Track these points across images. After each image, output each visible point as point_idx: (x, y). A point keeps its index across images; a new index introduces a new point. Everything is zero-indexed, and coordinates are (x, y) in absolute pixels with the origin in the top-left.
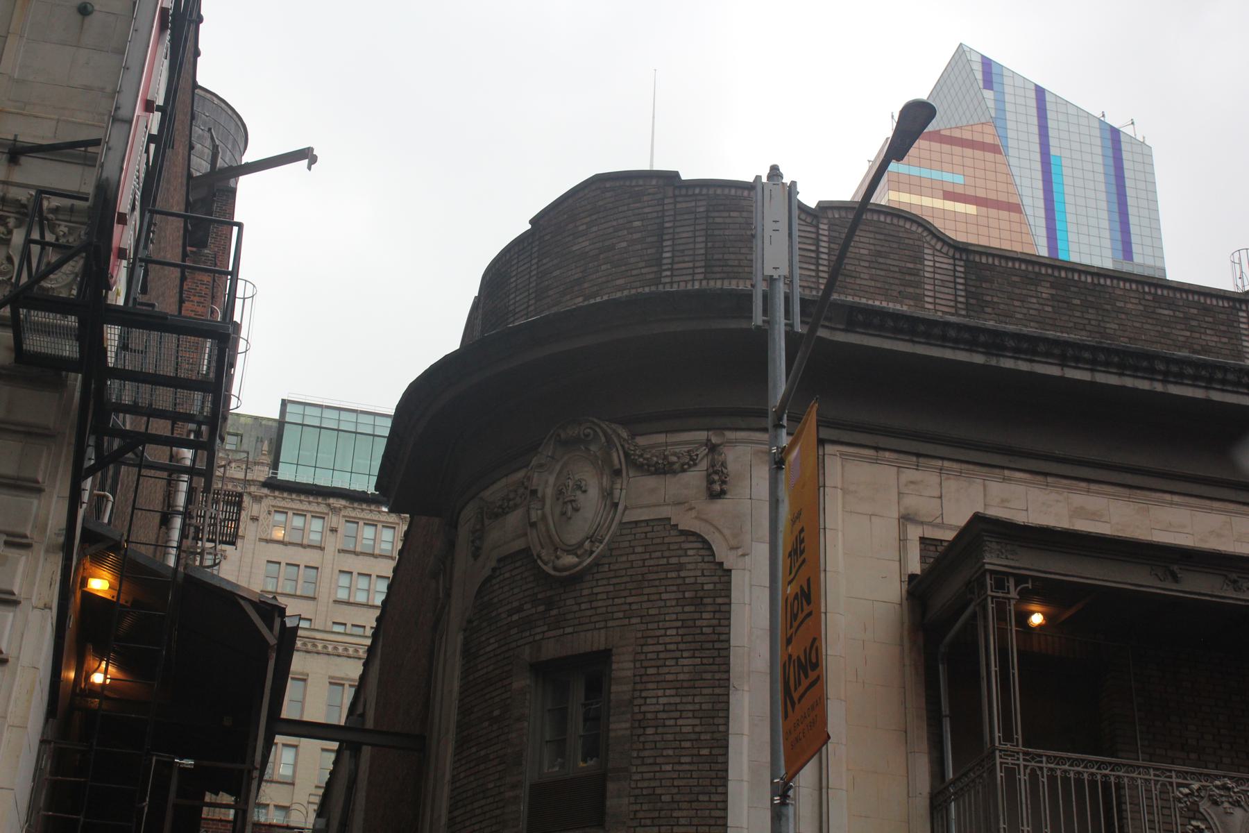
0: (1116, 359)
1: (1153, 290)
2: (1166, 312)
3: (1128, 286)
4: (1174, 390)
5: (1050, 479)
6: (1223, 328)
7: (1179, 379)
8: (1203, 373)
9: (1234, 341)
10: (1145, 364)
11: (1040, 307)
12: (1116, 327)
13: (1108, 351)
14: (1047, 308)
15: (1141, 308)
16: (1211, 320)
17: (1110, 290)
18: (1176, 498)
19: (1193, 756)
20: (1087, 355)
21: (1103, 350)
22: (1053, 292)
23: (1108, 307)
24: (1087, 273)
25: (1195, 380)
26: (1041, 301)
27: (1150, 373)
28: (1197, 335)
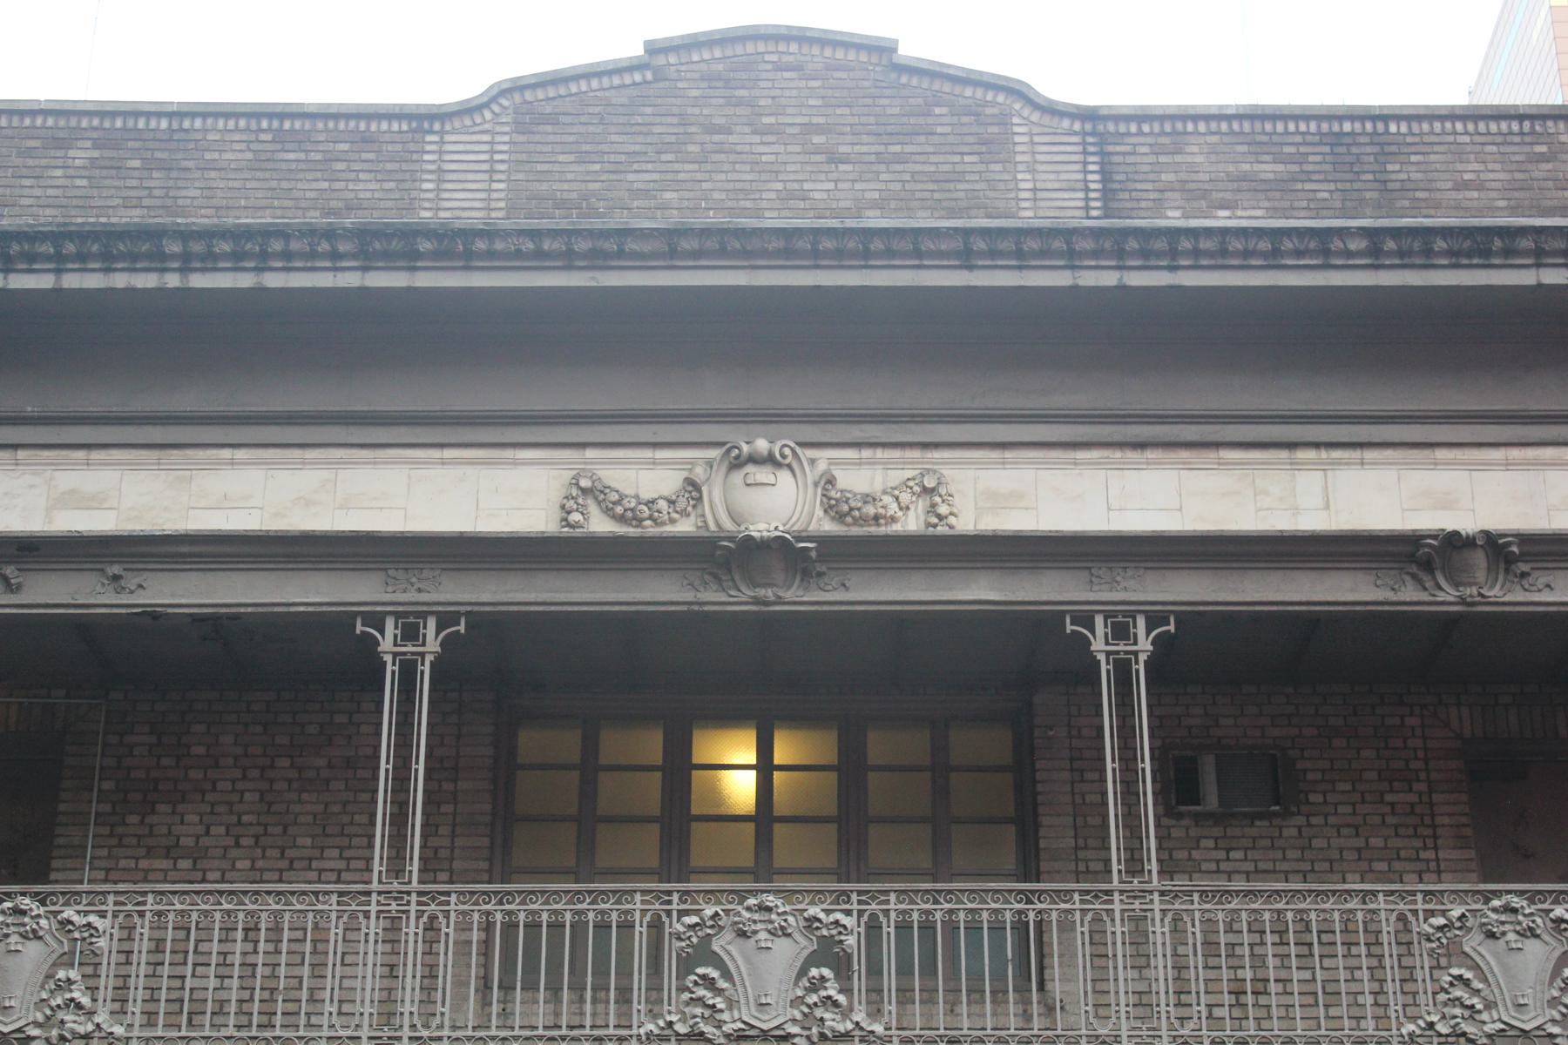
0: (95, 248)
1: (276, 124)
2: (292, 156)
3: (231, 124)
4: (199, 281)
5: (21, 454)
6: (389, 166)
7: (210, 262)
8: (249, 246)
9: (406, 185)
10: (145, 247)
11: (68, 182)
12: (198, 193)
13: (81, 236)
14: (79, 182)
15: (249, 156)
16: (371, 156)
17: (199, 136)
18: (240, 454)
19: (184, 864)
20: (47, 248)
21: (70, 236)
22: (96, 154)
23: (190, 164)
24: (159, 115)
25: (237, 260)
26: (71, 172)
27: (159, 261)
28: (341, 185)
